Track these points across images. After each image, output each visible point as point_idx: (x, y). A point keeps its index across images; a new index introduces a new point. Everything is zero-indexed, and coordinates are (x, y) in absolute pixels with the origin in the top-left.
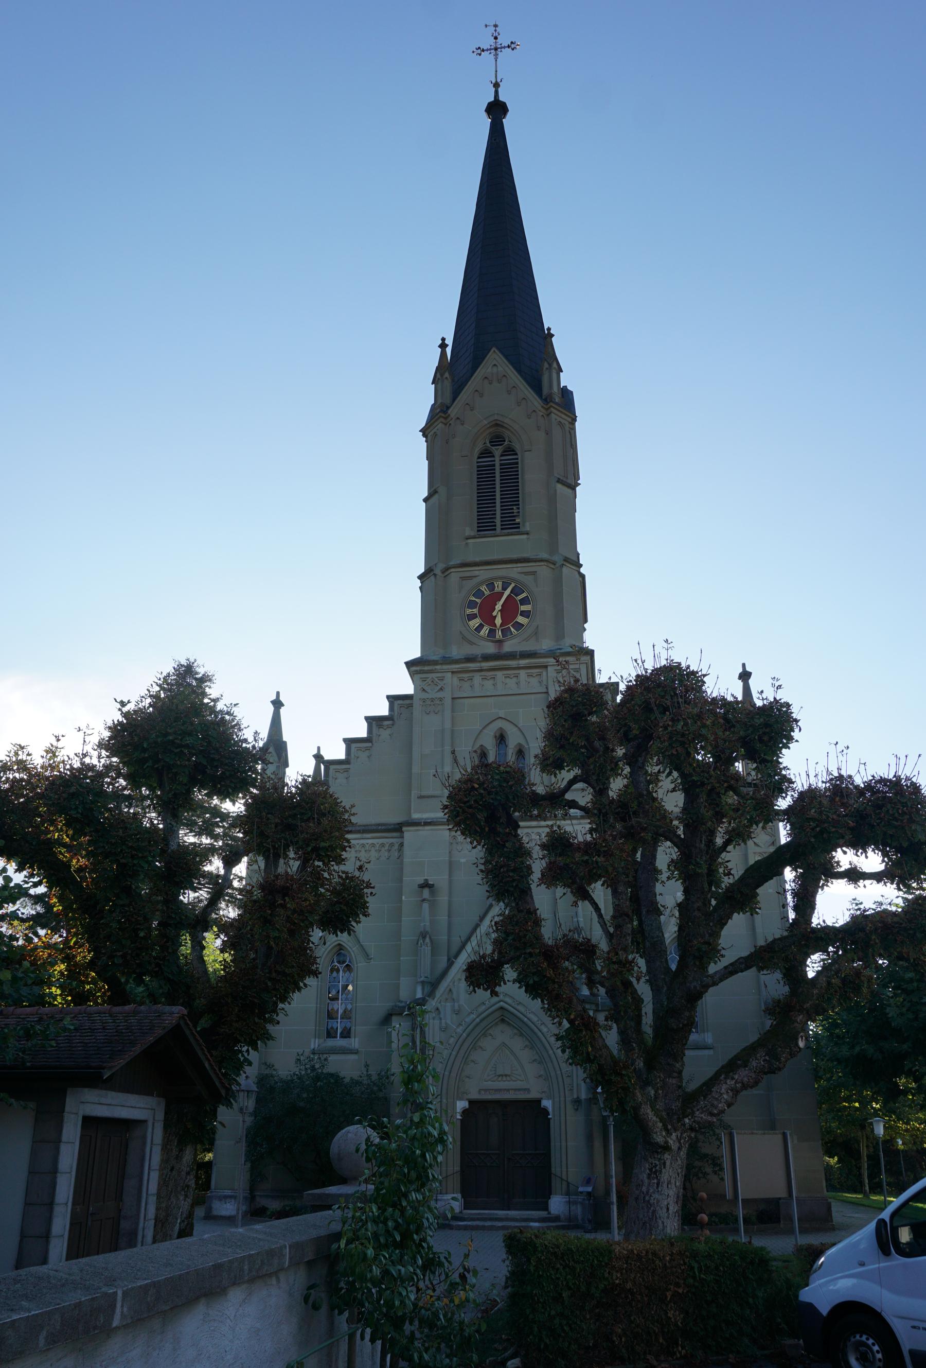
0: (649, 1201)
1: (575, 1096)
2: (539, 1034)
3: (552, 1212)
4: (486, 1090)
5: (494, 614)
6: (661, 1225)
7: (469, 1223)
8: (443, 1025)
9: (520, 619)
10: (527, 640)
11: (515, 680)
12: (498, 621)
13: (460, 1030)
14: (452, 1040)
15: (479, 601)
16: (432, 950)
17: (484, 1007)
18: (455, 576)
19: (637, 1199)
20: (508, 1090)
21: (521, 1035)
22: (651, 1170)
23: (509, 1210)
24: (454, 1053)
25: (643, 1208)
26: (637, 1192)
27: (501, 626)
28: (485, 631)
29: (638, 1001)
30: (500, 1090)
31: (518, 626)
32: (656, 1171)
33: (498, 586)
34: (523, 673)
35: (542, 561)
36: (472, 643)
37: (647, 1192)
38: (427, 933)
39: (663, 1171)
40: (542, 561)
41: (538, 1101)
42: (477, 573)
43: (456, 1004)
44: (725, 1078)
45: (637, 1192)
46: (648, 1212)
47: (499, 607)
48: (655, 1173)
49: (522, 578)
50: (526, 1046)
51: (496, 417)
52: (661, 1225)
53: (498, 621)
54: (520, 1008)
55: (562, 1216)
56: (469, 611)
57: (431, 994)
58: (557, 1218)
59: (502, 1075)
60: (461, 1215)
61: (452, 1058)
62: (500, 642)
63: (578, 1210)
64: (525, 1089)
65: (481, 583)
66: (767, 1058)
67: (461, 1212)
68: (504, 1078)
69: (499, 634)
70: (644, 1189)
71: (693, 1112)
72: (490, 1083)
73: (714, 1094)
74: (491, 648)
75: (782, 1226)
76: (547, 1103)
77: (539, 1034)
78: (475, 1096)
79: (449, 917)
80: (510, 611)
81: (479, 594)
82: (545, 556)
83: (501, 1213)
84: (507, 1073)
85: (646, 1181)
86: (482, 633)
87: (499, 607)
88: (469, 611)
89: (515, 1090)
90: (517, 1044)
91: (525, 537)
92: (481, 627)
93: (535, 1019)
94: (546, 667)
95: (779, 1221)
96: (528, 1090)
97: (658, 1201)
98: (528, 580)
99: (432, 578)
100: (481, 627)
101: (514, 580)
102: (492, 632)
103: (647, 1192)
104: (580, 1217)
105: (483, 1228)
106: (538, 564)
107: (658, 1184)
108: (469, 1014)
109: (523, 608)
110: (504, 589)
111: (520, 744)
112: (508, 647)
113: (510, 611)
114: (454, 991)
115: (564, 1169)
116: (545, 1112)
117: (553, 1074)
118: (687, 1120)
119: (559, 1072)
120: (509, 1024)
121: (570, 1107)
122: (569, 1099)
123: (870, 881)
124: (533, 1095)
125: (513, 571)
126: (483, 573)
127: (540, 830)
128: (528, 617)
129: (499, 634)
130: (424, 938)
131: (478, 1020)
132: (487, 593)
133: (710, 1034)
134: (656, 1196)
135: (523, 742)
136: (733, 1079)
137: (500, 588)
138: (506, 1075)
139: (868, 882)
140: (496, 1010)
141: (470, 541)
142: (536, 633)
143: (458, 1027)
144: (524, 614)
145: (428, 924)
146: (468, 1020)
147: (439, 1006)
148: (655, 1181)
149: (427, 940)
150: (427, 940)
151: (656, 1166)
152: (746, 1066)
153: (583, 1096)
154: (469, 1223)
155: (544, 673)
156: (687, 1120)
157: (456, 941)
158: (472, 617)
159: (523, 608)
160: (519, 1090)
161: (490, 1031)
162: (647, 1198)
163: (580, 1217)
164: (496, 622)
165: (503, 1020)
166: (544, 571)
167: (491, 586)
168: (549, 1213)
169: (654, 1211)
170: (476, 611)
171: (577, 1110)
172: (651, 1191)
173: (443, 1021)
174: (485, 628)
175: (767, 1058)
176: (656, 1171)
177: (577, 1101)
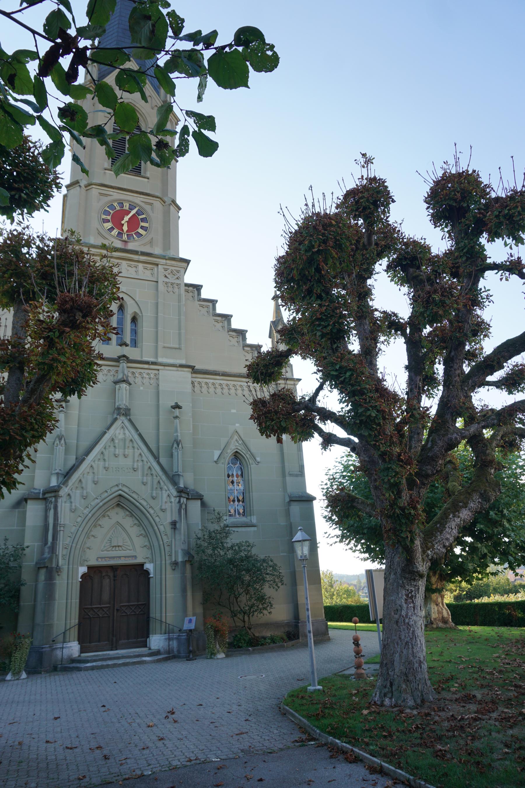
0: (408, 623)
1: (173, 560)
2: (148, 515)
3: (152, 648)
4: (102, 558)
5: (123, 222)
6: (419, 643)
7: (94, 664)
8: (73, 507)
9: (140, 231)
10: (144, 245)
11: (134, 269)
12: (125, 228)
13: (86, 511)
14: (79, 519)
15: (112, 212)
16: (66, 449)
17: (106, 494)
18: (95, 191)
19: (397, 622)
20: (120, 557)
21: (132, 515)
22: (407, 595)
23: (116, 650)
24: (81, 529)
25: (404, 630)
26: (397, 616)
27: (127, 231)
28: (115, 232)
29: (520, 427)
30: (114, 557)
31: (139, 235)
32: (412, 596)
33: (126, 206)
34: (141, 265)
35: (157, 197)
36: (105, 238)
37: (407, 615)
38: (63, 436)
39: (417, 595)
40: (157, 197)
41: (142, 565)
42: (111, 193)
43: (85, 491)
44: (454, 517)
45: (397, 616)
46: (409, 633)
47: (126, 218)
48: (411, 598)
49: (142, 205)
50: (135, 524)
51: (130, 101)
52: (419, 643)
53: (125, 228)
54: (134, 495)
55: (162, 650)
56: (104, 217)
57: (65, 483)
58: (158, 653)
59: (116, 546)
60: (79, 658)
61: (79, 532)
62: (125, 242)
63: (175, 644)
64: (133, 556)
65: (115, 201)
66: (480, 500)
67: (79, 656)
68: (117, 548)
69: (125, 237)
70: (404, 613)
71: (434, 545)
72: (105, 552)
73: (447, 529)
74: (118, 244)
75: (300, 641)
76: (149, 566)
77: (148, 515)
78: (93, 562)
79: (78, 426)
80: (134, 223)
81: (112, 207)
82: (158, 194)
83: (111, 652)
84: (119, 544)
85: (405, 606)
86: (113, 233)
87: (126, 218)
88: (104, 217)
89: (125, 557)
90: (128, 522)
91: (146, 180)
92: (111, 229)
93: (145, 504)
94: (157, 265)
95: (298, 638)
96: (135, 557)
97: (415, 622)
98: (147, 208)
99: (78, 188)
100: (111, 229)
101: (139, 205)
102: (120, 234)
103: (407, 615)
104: (175, 650)
105: (108, 666)
106: (154, 199)
107: (414, 608)
108: (94, 500)
109: (143, 224)
110: (131, 209)
111: (135, 312)
112: (131, 246)
113: (134, 223)
114: (83, 480)
115: (164, 615)
116: (147, 572)
117: (156, 544)
118: (429, 552)
119: (161, 543)
120: (123, 507)
121: (169, 568)
122: (168, 562)
123: (492, 387)
124: (139, 560)
125: (138, 199)
126: (116, 195)
127: (150, 371)
128: (146, 231)
129: (125, 237)
130: (60, 439)
131: (101, 504)
132: (118, 208)
133: (255, 517)
134: (414, 618)
135: (138, 311)
136: (459, 517)
137: (127, 208)
138: (119, 546)
139: (491, 387)
140: (114, 498)
141: (107, 171)
142: (151, 242)
143: (85, 509)
144: (142, 227)
145: (63, 429)
146: (93, 503)
147: (71, 492)
148: (412, 605)
149: (63, 441)
150: (63, 441)
151: (412, 591)
152: (466, 507)
153: (180, 559)
154: (94, 664)
155: (156, 269)
156: (429, 552)
157: (85, 444)
158: (106, 221)
159: (143, 224)
160: (128, 557)
161: (108, 513)
162: (407, 621)
163: (175, 650)
164: (124, 228)
165: (118, 505)
166: (157, 204)
167: (121, 204)
168: (150, 649)
169: (414, 631)
170: (109, 218)
171: (174, 570)
172: (410, 614)
173: (73, 504)
174: (115, 231)
175: (480, 500)
176: (412, 596)
177: (175, 564)
